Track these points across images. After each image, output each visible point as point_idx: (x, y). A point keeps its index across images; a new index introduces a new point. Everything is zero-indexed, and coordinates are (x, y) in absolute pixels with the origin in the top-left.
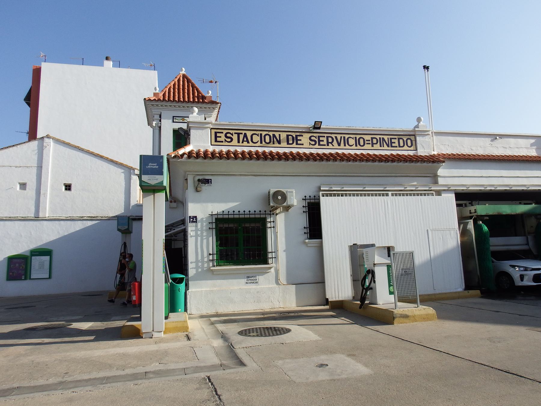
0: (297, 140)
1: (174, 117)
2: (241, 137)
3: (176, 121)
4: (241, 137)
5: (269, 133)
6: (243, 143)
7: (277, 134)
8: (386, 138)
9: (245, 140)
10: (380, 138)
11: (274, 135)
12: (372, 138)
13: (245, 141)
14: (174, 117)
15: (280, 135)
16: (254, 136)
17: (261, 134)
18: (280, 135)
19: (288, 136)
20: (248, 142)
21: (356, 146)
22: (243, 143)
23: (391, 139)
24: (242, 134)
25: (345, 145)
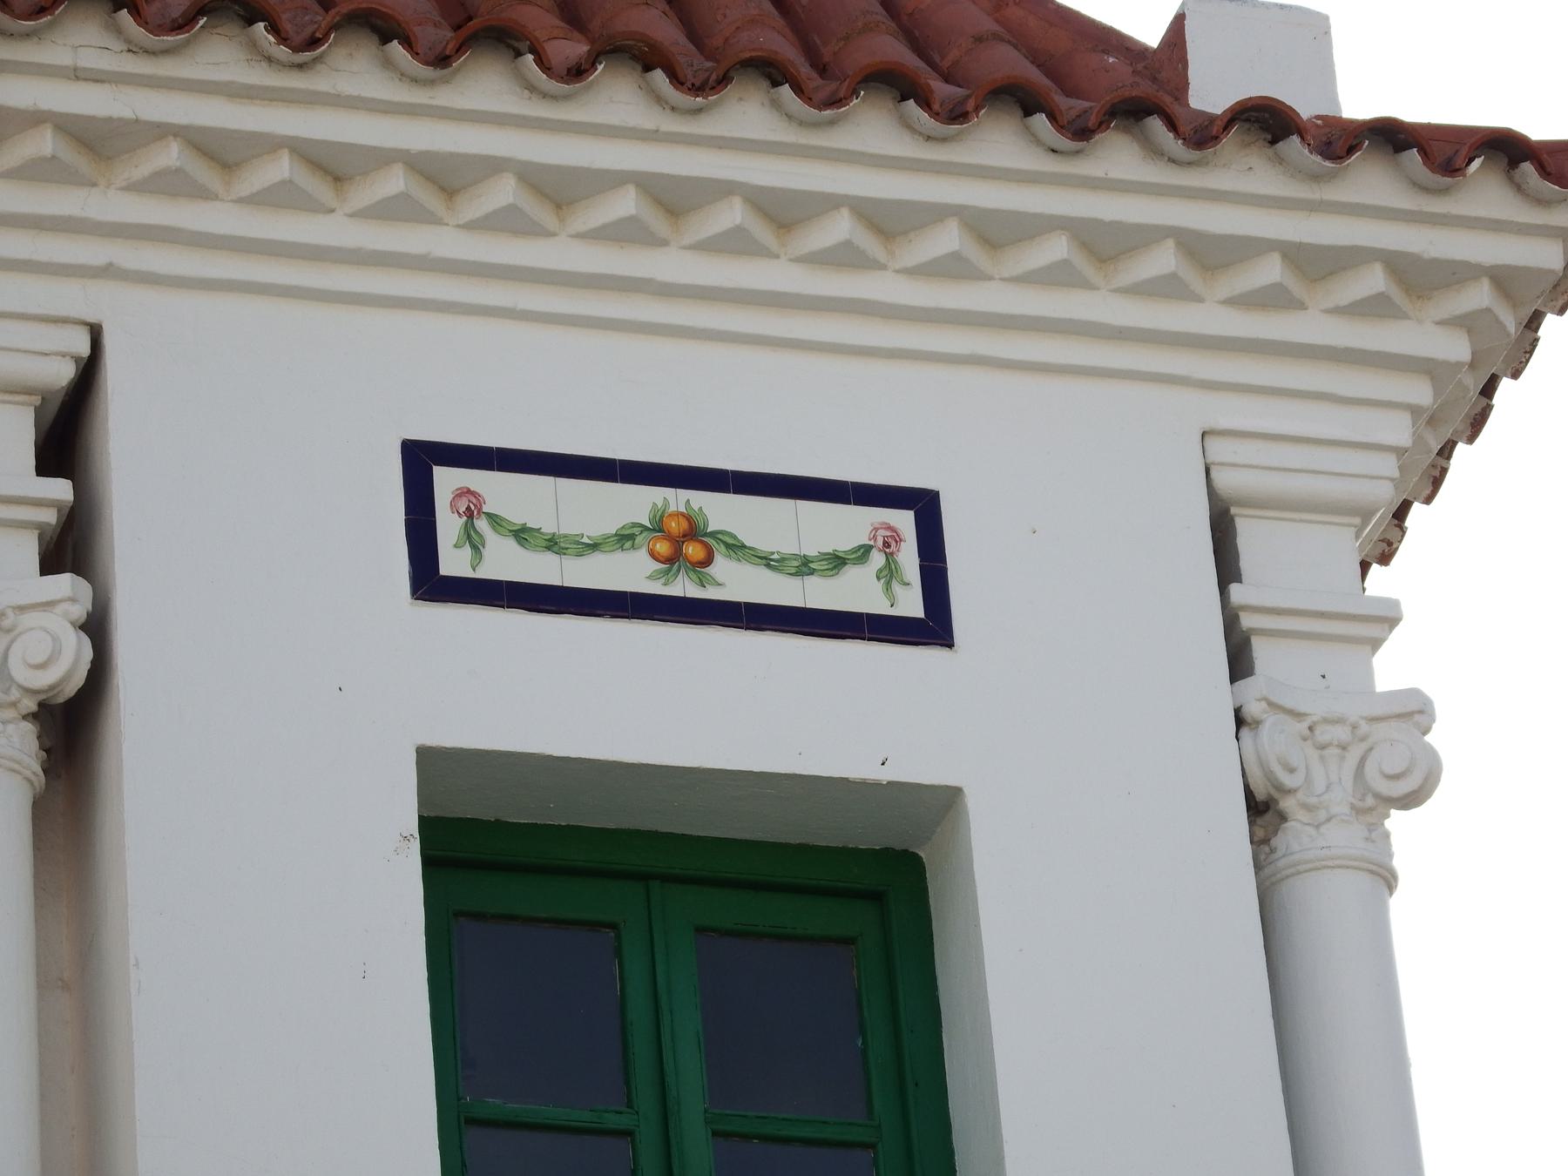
1: (446, 480)
14: (446, 480)
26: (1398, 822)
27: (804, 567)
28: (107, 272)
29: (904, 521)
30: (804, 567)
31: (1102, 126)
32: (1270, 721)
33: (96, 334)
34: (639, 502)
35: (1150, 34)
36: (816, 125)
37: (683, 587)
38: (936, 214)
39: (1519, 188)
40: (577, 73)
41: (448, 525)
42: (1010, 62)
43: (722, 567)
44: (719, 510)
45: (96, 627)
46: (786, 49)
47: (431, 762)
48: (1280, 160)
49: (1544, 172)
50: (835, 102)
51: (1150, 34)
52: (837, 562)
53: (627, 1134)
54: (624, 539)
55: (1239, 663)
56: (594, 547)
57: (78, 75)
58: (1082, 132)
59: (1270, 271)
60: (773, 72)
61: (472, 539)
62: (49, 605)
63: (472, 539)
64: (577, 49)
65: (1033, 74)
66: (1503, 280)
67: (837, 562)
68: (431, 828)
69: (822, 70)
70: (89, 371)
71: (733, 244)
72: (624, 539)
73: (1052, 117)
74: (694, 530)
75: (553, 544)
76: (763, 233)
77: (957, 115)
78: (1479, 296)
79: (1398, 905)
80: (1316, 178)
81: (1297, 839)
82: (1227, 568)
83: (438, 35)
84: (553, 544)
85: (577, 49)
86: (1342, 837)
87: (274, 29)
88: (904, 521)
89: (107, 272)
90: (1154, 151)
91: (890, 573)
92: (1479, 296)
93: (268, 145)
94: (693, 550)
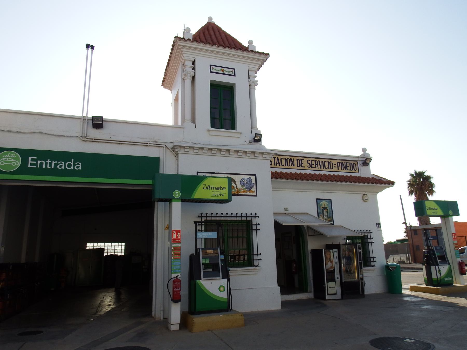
0: (302, 164)
2: (276, 159)
3: (214, 71)
4: (276, 159)
5: (288, 158)
6: (277, 165)
7: (292, 158)
8: (344, 162)
9: (278, 163)
10: (341, 162)
11: (291, 159)
12: (338, 162)
13: (278, 164)
14: (212, 67)
15: (293, 159)
16: (282, 159)
17: (285, 158)
18: (293, 159)
19: (297, 160)
20: (280, 165)
21: (329, 169)
22: (277, 165)
23: (346, 163)
24: (276, 158)
25: (323, 168)
26: (256, 86)
27: (229, 72)
28: (196, 55)
29: (234, 70)
30: (229, 72)
31: (244, 51)
32: (250, 81)
33: (195, 58)
34: (221, 68)
35: (247, 47)
36: (230, 50)
37: (223, 73)
38: (236, 55)
39: (264, 55)
40: (219, 46)
41: (212, 69)
42: (240, 47)
43: (225, 72)
44: (225, 69)
45: (195, 73)
46: (229, 46)
47: (210, 80)
48: (253, 53)
49: (265, 55)
50: (231, 49)
51: (247, 47)
52: (230, 72)
53: (219, 99)
54: (220, 70)
55: (249, 78)
56: (219, 70)
57: (195, 45)
58: (243, 51)
59: (252, 59)
60: (228, 47)
61: (213, 70)
62: (192, 72)
63: (213, 70)
64: (219, 45)
65: (241, 48)
66: (263, 60)
67: (230, 72)
68: (210, 84)
69: (231, 47)
70: (195, 60)
71: (226, 56)
72: (220, 70)
73: (242, 50)
74: (223, 70)
75: (217, 70)
76: (227, 55)
77: (237, 50)
78: (262, 61)
79: (255, 90)
80: (254, 54)
81: (251, 87)
82: (249, 74)
83: (212, 44)
84: (217, 70)
85: (219, 45)
86: (253, 87)
87: (204, 43)
88: (234, 70)
89: (196, 55)
90: (247, 52)
91: (233, 73)
92: (262, 61)
93: (204, 49)
94: (223, 71)
